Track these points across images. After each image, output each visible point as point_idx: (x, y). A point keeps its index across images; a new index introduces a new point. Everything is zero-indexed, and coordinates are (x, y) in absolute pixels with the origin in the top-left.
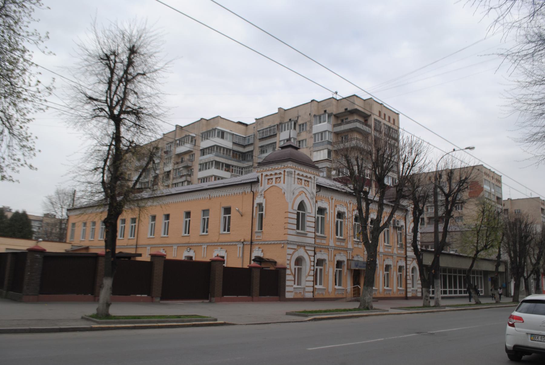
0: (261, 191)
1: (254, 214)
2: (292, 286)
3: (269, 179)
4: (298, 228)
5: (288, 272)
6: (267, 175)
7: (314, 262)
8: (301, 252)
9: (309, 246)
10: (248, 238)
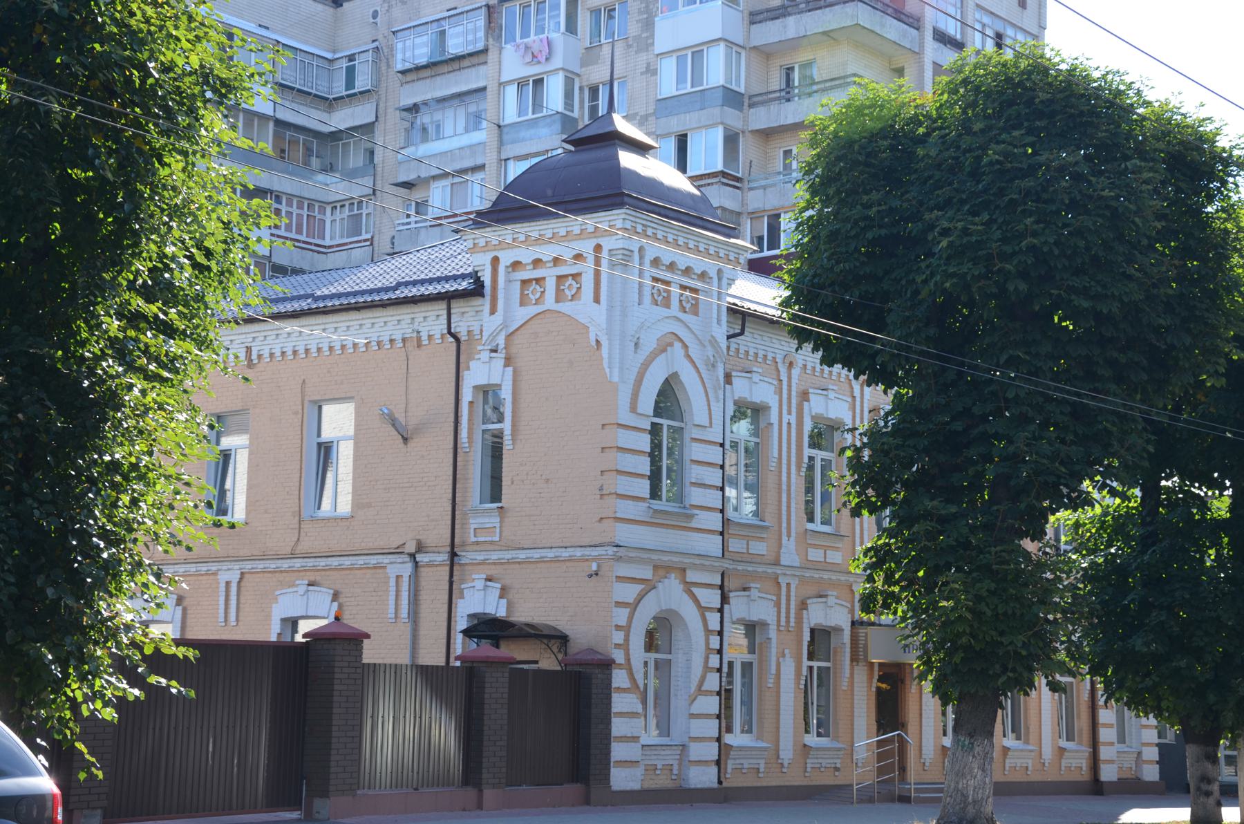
0: (494, 335)
1: (464, 433)
2: (635, 739)
3: (525, 283)
4: (655, 493)
5: (619, 678)
6: (516, 265)
8: (670, 595)
9: (703, 568)
10: (439, 535)
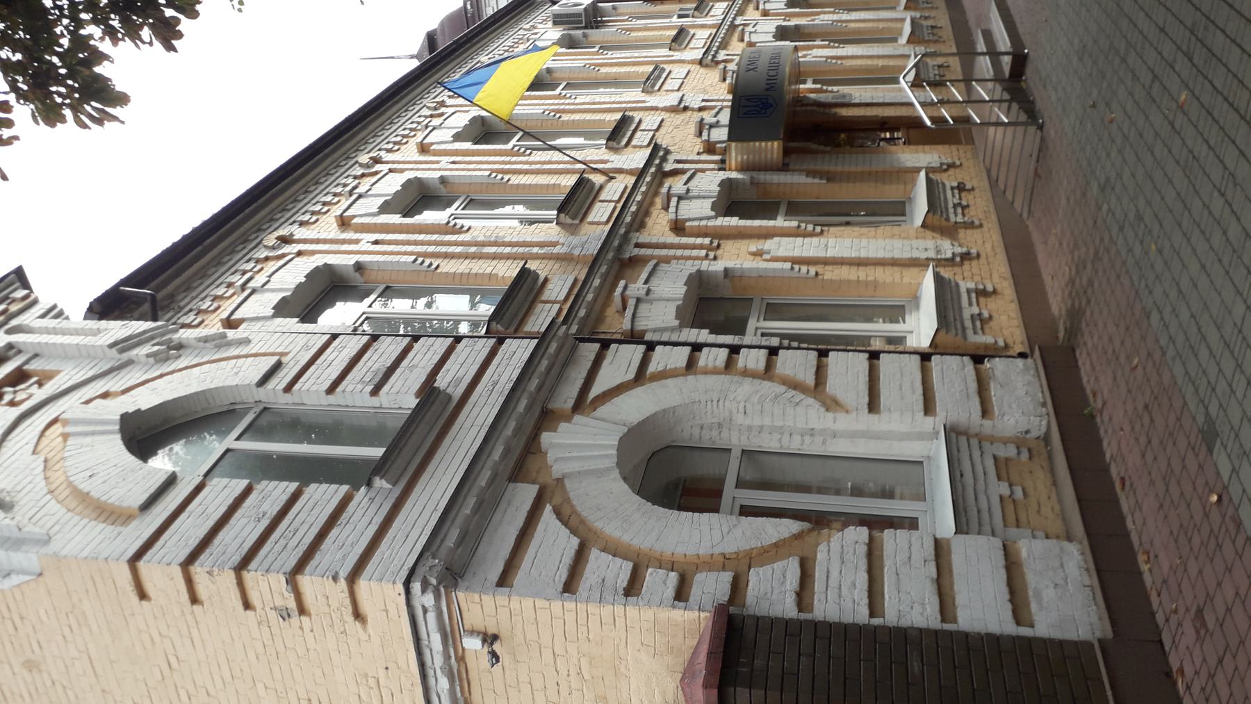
2: (940, 549)
5: (771, 593)
7: (697, 347)
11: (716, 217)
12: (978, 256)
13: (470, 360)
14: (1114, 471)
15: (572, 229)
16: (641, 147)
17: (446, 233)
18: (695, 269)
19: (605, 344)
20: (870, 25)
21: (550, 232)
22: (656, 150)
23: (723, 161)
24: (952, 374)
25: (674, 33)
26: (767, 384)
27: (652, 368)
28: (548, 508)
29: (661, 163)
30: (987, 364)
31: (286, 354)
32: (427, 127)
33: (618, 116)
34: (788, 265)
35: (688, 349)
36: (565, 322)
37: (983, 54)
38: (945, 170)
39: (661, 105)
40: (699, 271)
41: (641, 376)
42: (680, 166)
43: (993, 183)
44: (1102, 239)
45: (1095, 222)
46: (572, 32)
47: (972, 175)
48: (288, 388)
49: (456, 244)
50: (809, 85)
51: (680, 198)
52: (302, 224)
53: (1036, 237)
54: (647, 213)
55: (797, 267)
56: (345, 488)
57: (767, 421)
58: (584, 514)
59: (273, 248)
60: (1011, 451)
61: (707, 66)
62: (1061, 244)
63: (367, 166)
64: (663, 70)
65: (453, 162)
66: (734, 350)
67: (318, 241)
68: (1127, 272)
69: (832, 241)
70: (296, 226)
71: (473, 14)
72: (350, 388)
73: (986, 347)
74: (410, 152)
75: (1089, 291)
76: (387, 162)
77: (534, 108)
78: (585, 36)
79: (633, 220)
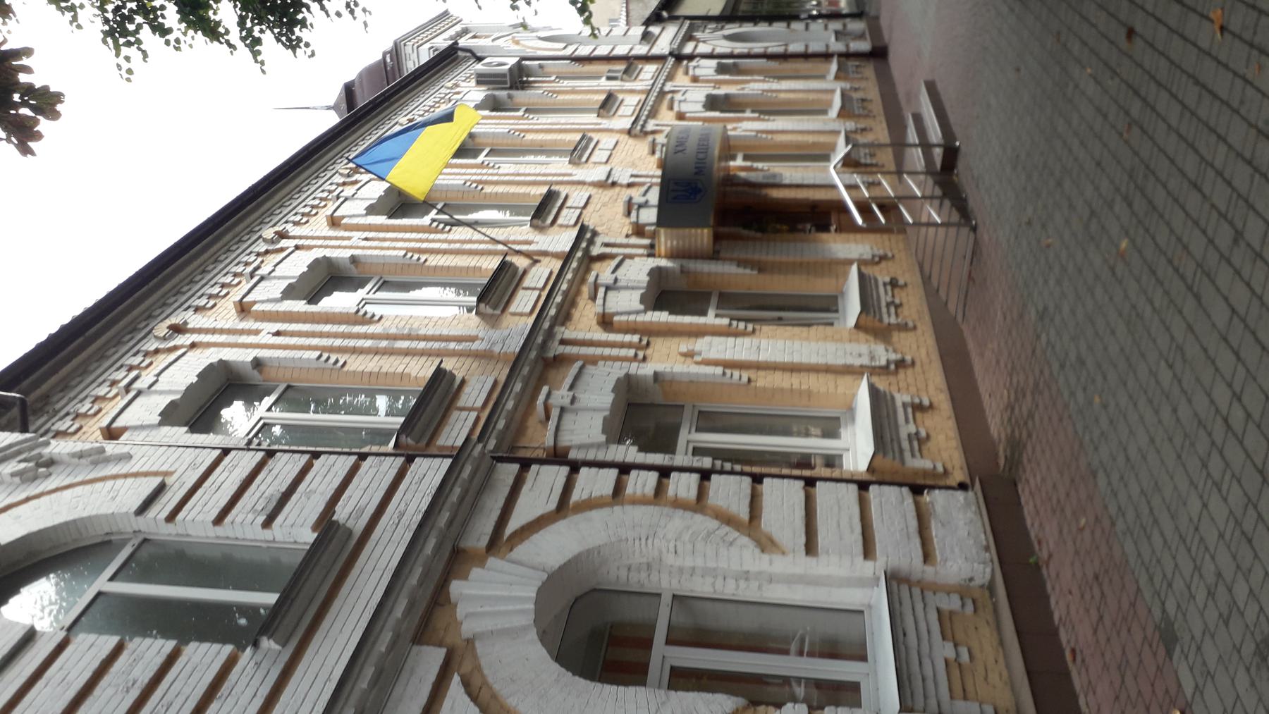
7: (625, 469)
11: (645, 311)
12: (913, 363)
13: (374, 485)
14: (1063, 636)
15: (492, 321)
16: (567, 226)
17: (356, 323)
18: (623, 372)
19: (525, 464)
20: (801, 96)
21: (471, 324)
22: (585, 234)
23: (652, 246)
24: (890, 504)
25: (603, 97)
26: (699, 518)
27: (576, 496)
28: (456, 679)
29: (588, 246)
30: (927, 497)
31: (171, 473)
32: (338, 197)
33: (544, 190)
34: (719, 370)
35: (613, 473)
36: (480, 439)
37: (915, 145)
38: (878, 263)
39: (589, 179)
40: (628, 376)
41: (564, 507)
42: (608, 250)
43: (926, 280)
44: (1042, 372)
45: (1034, 351)
46: (497, 93)
47: (904, 269)
48: (171, 517)
49: (365, 336)
50: (739, 162)
51: (608, 288)
52: (197, 309)
53: (971, 345)
54: (573, 304)
55: (728, 372)
56: (228, 649)
57: (699, 562)
58: (496, 687)
59: (164, 339)
60: (953, 603)
61: (635, 136)
62: (998, 362)
63: (272, 242)
64: (591, 139)
65: (366, 239)
66: (664, 472)
67: (213, 331)
68: (1070, 417)
69: (764, 343)
70: (191, 312)
71: (392, 68)
72: (239, 520)
73: (925, 473)
74: (319, 226)
75: (1030, 423)
76: (294, 237)
77: (457, 178)
78: (510, 97)
79: (558, 313)
